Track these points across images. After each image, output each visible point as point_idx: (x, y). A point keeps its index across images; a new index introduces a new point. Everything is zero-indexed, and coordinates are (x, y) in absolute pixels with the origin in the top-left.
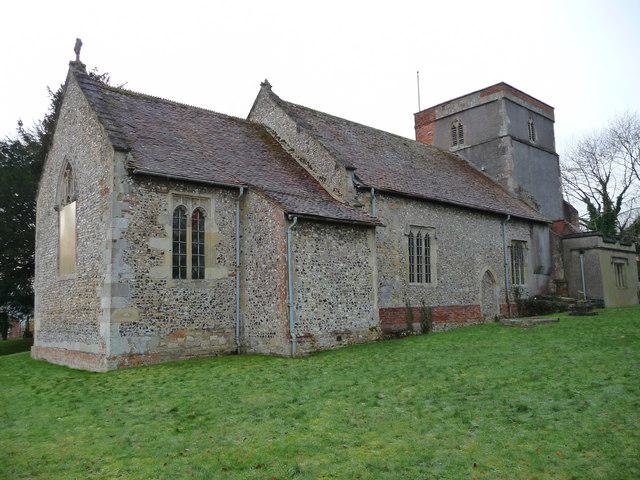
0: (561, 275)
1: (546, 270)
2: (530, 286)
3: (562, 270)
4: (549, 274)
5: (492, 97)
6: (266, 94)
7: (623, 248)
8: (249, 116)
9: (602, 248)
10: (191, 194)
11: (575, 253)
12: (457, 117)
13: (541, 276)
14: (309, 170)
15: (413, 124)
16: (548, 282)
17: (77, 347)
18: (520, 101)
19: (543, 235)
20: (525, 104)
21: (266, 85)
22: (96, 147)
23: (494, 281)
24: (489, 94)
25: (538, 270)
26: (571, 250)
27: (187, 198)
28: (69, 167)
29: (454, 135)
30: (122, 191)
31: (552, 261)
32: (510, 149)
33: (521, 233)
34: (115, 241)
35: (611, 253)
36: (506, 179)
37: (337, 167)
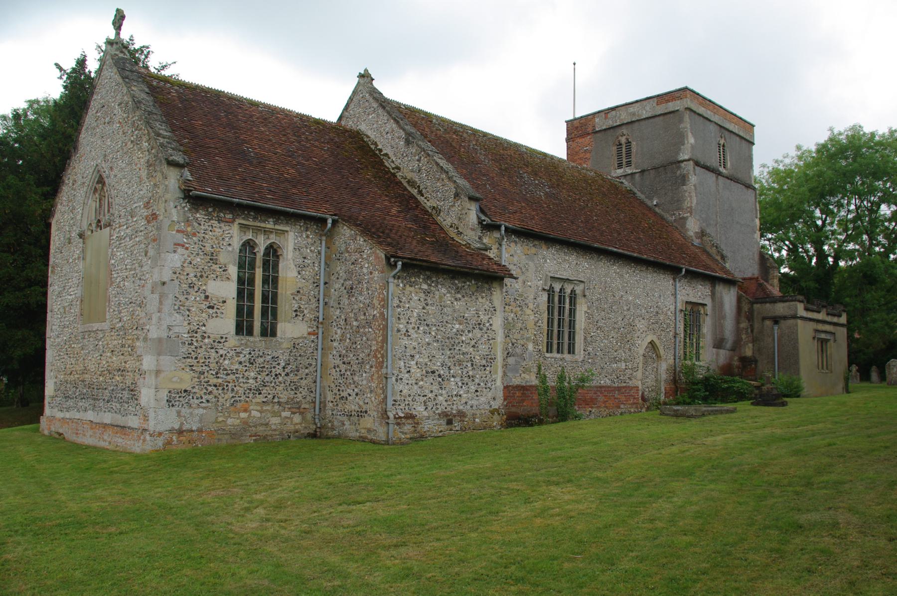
0: (748, 352)
1: (729, 345)
2: (709, 359)
3: (750, 345)
4: (733, 349)
5: (672, 106)
6: (365, 89)
7: (829, 319)
8: (340, 118)
9: (802, 318)
10: (263, 225)
11: (768, 323)
12: (624, 130)
13: (722, 352)
14: (419, 197)
15: (565, 136)
16: (731, 358)
17: (107, 418)
18: (708, 114)
19: (729, 297)
20: (715, 118)
21: (365, 77)
22: (141, 158)
23: (659, 357)
24: (668, 101)
25: (719, 344)
26: (764, 319)
27: (257, 230)
28: (101, 181)
29: (619, 154)
30: (175, 218)
31: (738, 331)
32: (693, 179)
33: (699, 293)
34: (164, 283)
35: (813, 326)
36: (685, 219)
37: (457, 195)
